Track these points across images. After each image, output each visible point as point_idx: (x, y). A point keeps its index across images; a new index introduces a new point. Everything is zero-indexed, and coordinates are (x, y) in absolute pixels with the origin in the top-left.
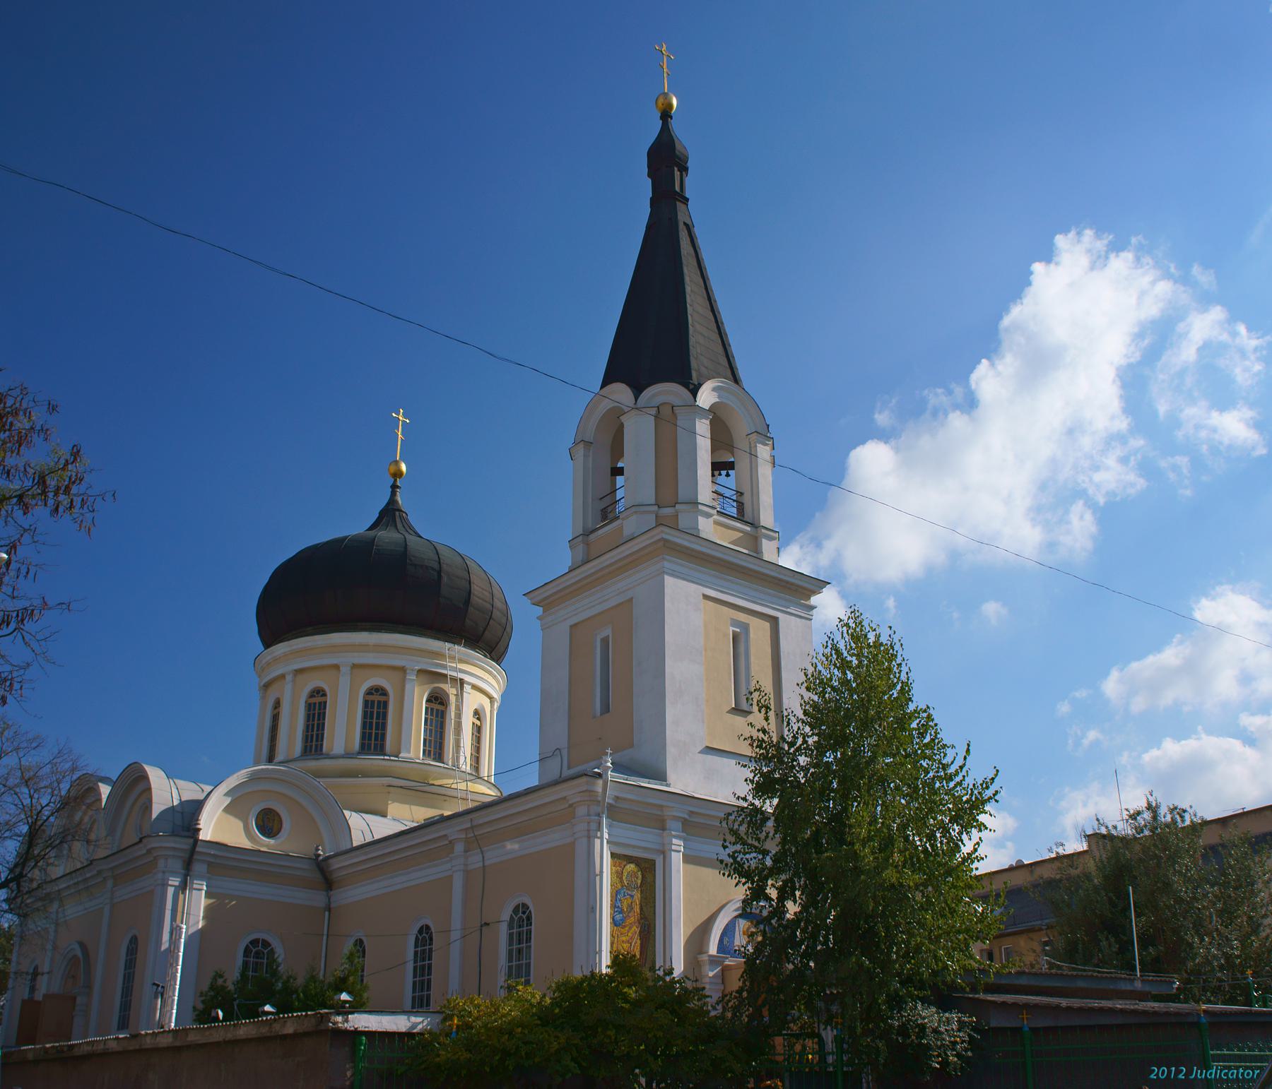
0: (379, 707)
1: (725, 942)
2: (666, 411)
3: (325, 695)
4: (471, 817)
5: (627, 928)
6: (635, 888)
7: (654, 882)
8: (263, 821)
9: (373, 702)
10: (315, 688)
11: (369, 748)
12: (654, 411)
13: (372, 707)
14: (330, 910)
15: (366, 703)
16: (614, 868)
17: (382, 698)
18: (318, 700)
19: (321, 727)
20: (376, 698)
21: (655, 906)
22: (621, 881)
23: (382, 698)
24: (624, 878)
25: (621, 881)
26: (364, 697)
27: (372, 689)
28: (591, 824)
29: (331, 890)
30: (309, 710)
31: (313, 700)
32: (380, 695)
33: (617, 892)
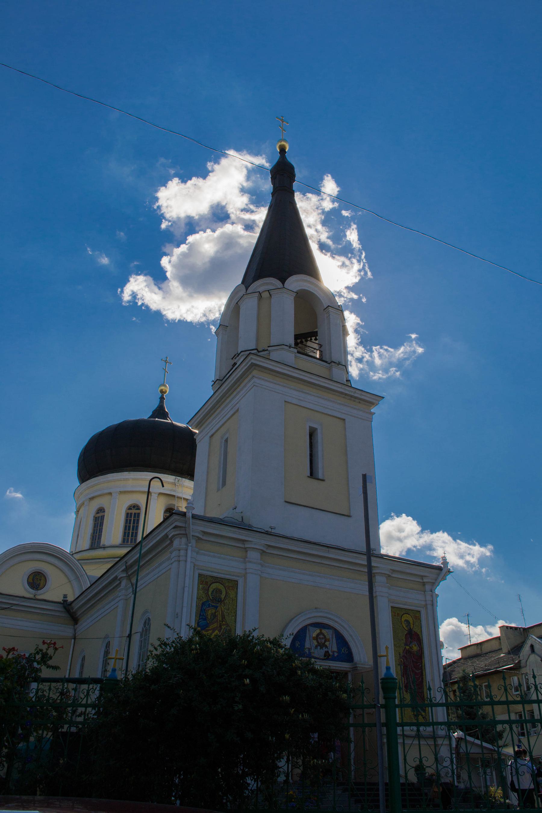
0: (135, 517)
1: (297, 644)
2: (265, 295)
3: (104, 512)
4: (125, 561)
5: (211, 632)
6: (219, 601)
7: (236, 597)
8: (33, 580)
9: (131, 514)
10: (100, 508)
11: (128, 542)
12: (257, 294)
13: (131, 517)
14: (75, 639)
15: (127, 514)
16: (201, 586)
17: (137, 511)
18: (100, 515)
19: (101, 531)
20: (134, 511)
21: (236, 615)
22: (207, 594)
23: (137, 511)
24: (210, 593)
25: (207, 594)
26: (126, 511)
27: (131, 506)
28: (181, 551)
29: (77, 624)
30: (96, 521)
31: (98, 515)
32: (136, 509)
33: (203, 604)
